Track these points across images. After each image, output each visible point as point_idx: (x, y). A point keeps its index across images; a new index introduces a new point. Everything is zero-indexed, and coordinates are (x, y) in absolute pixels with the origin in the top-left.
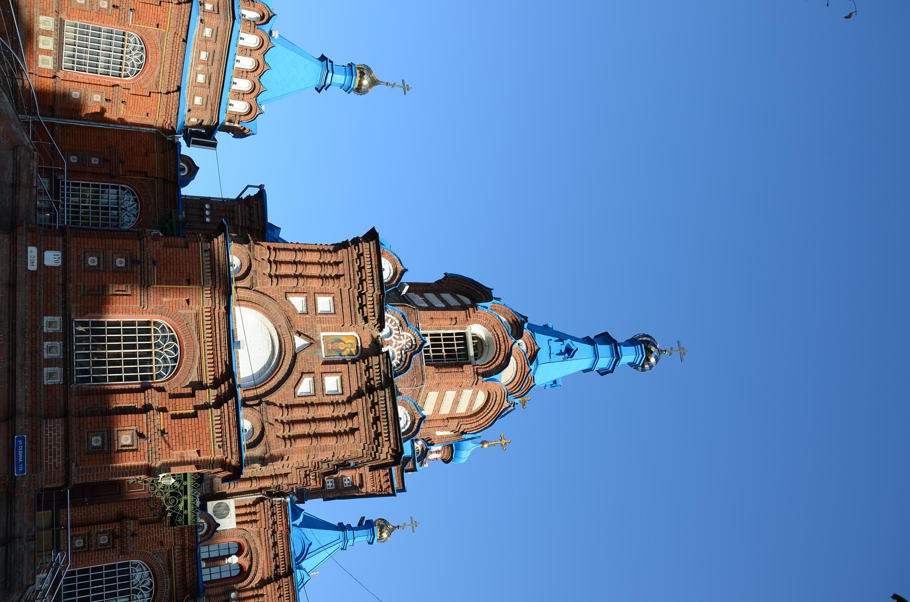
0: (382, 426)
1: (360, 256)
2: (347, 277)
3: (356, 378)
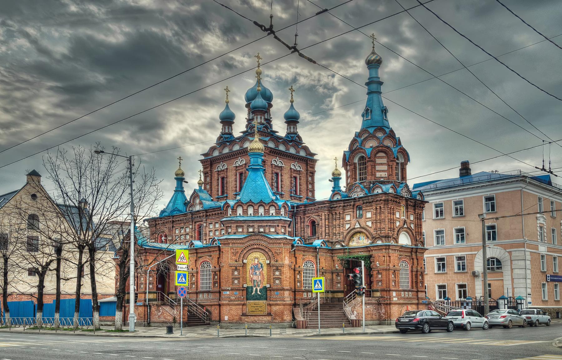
0: (422, 206)
1: (391, 200)
2: (394, 206)
3: (411, 210)
